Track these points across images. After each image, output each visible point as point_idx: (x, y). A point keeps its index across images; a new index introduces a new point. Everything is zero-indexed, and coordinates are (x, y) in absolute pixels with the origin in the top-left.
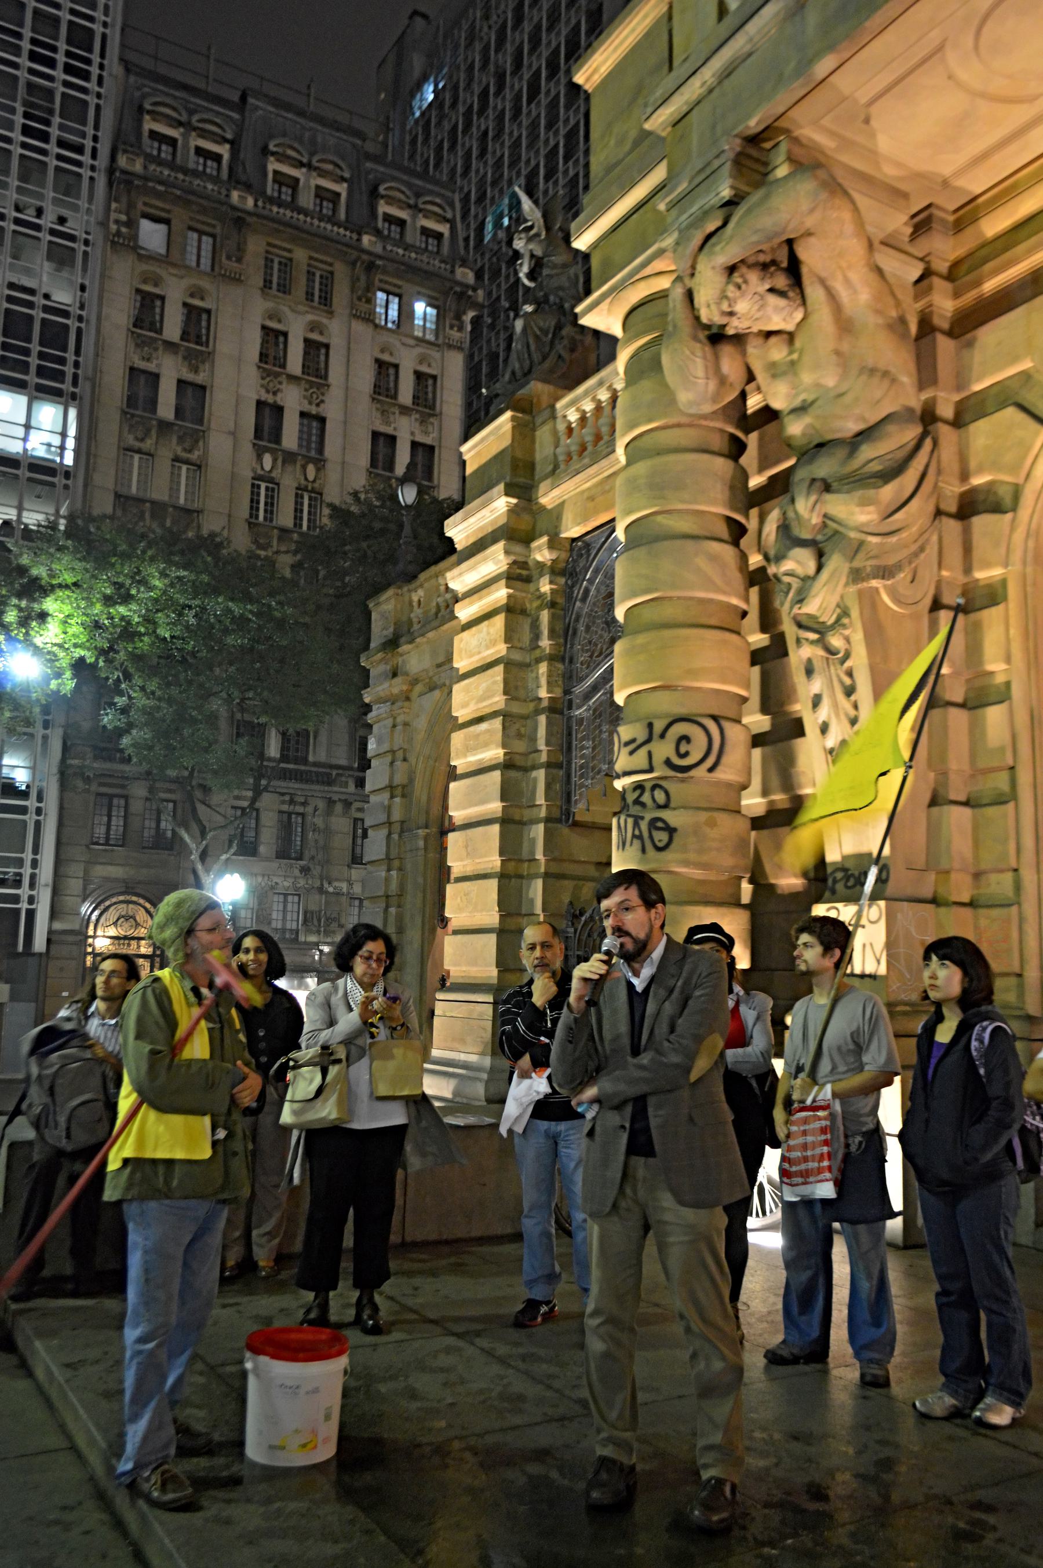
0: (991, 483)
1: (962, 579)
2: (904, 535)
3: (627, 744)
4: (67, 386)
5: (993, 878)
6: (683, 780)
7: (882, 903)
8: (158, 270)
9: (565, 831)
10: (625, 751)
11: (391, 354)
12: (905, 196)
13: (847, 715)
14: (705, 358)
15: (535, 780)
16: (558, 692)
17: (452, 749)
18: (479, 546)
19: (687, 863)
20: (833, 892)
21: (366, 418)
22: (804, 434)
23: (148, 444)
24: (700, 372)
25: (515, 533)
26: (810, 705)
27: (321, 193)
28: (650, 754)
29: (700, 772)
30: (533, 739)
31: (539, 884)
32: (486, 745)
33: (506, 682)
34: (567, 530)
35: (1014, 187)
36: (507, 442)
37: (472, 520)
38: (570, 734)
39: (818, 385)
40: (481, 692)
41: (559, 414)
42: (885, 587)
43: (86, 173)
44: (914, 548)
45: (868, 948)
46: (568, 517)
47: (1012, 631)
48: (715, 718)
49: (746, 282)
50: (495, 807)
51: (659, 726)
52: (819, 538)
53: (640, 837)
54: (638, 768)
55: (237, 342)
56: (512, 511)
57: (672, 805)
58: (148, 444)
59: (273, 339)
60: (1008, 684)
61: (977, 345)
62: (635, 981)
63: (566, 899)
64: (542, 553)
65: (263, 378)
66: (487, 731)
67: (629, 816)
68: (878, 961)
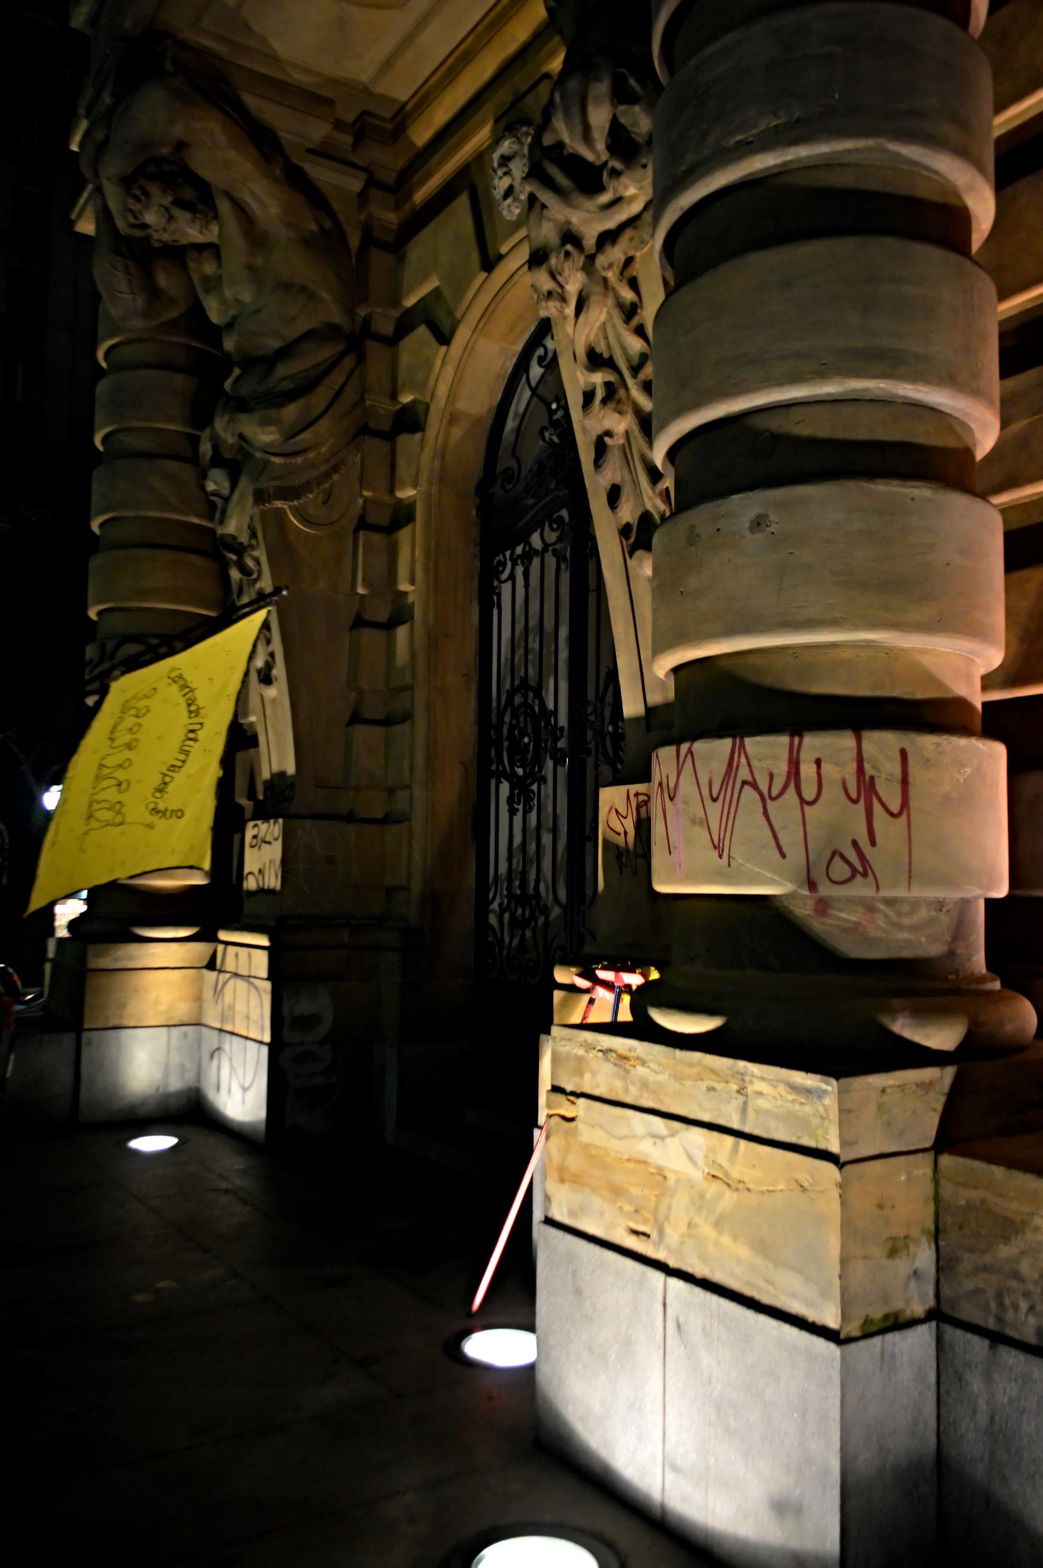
0: (414, 402)
2: (311, 455)
14: (128, 272)
24: (123, 287)
35: (426, 96)
42: (290, 507)
44: (323, 469)
47: (417, 552)
49: (146, 194)
51: (110, 646)
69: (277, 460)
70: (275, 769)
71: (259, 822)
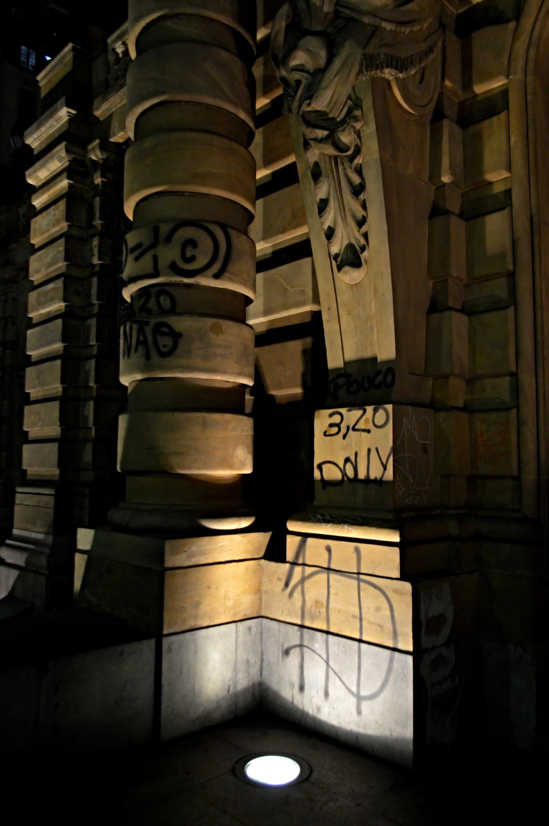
1: (461, 95)
5: (488, 383)
7: (390, 407)
10: (131, 257)
13: (354, 217)
15: (89, 326)
17: (30, 305)
18: (49, 148)
25: (74, 137)
26: (316, 210)
28: (155, 258)
30: (88, 296)
31: (92, 404)
32: (51, 301)
33: (67, 251)
34: (115, 135)
36: (68, 69)
37: (43, 129)
41: (110, 48)
42: (397, 79)
45: (373, 453)
46: (115, 125)
47: (513, 139)
50: (58, 346)
51: (164, 229)
52: (330, 30)
54: (144, 273)
56: (72, 120)
60: (508, 193)
66: (54, 289)
67: (134, 322)
68: (385, 468)
69: (388, 26)
70: (350, 355)
71: (343, 411)
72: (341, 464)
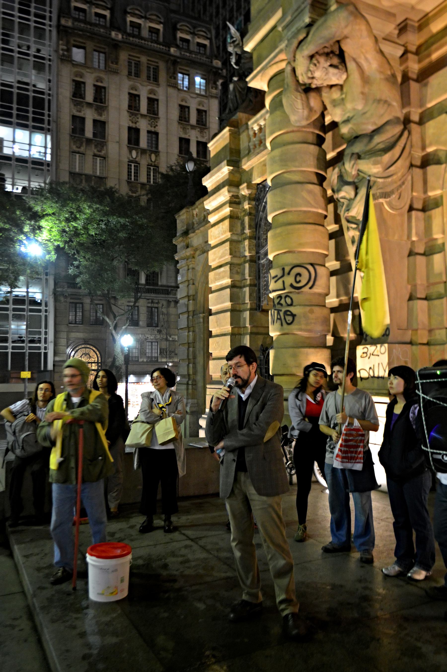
0: (436, 151)
1: (423, 196)
2: (394, 177)
3: (274, 278)
4: (45, 126)
5: (437, 332)
6: (298, 293)
7: (386, 345)
8: (82, 71)
9: (259, 314)
11: (186, 102)
12: (394, 15)
14: (302, 100)
15: (245, 292)
16: (254, 253)
17: (210, 280)
18: (217, 189)
19: (301, 330)
20: (366, 340)
21: (176, 132)
22: (349, 132)
23: (82, 149)
25: (232, 183)
27: (151, 30)
28: (283, 282)
29: (306, 289)
30: (243, 274)
32: (223, 278)
33: (231, 249)
34: (255, 180)
36: (227, 141)
37: (214, 177)
38: (259, 271)
39: (354, 109)
40: (220, 254)
41: (250, 127)
42: (386, 202)
43: (47, 28)
44: (399, 183)
46: (255, 174)
48: (312, 265)
49: (319, 62)
50: (228, 304)
51: (287, 269)
52: (356, 180)
53: (280, 319)
54: (278, 288)
55: (118, 101)
56: (231, 173)
57: (294, 304)
58: (82, 149)
59: (134, 98)
61: (429, 85)
62: (242, 396)
63: (260, 343)
64: (244, 191)
65: (130, 117)
66: (224, 271)
67: (275, 310)
68: (385, 371)
69: (380, 180)
71: (368, 346)
72: (368, 370)
